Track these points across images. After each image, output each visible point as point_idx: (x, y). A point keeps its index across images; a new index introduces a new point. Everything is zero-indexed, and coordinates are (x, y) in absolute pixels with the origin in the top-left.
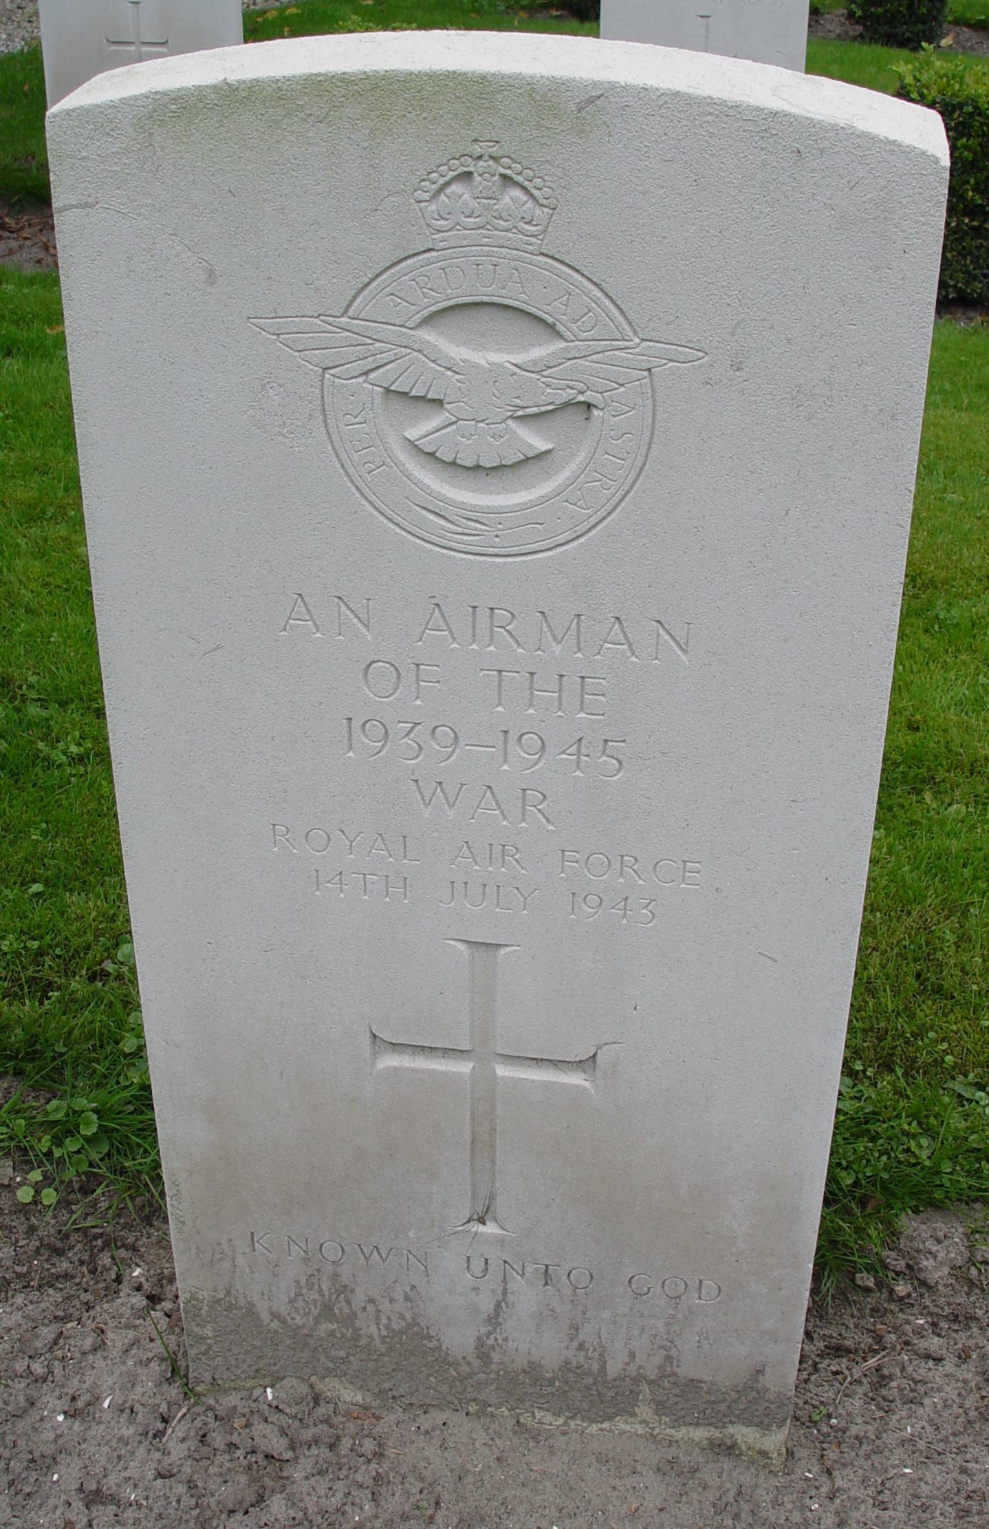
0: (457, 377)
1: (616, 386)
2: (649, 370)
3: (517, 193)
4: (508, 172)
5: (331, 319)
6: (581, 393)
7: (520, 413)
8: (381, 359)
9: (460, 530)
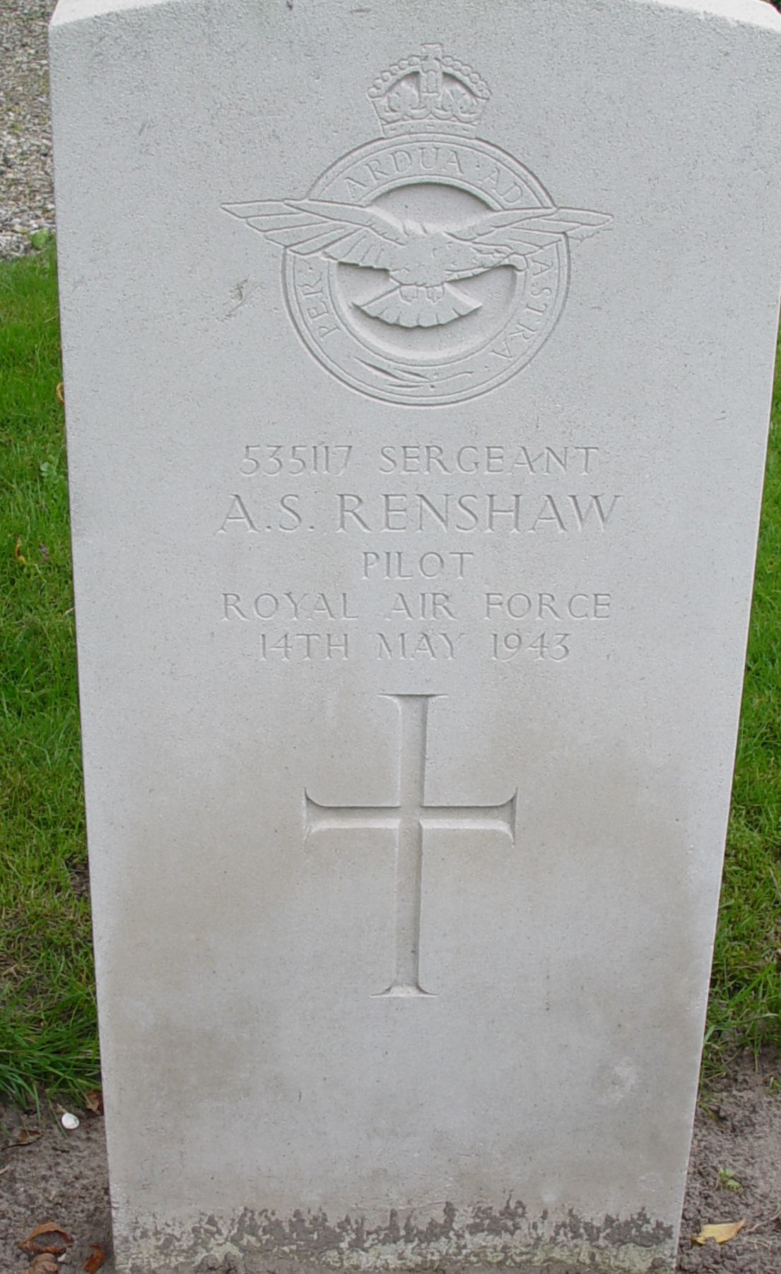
3: (458, 87)
4: (450, 70)
5: (292, 202)
7: (455, 276)
8: (337, 234)
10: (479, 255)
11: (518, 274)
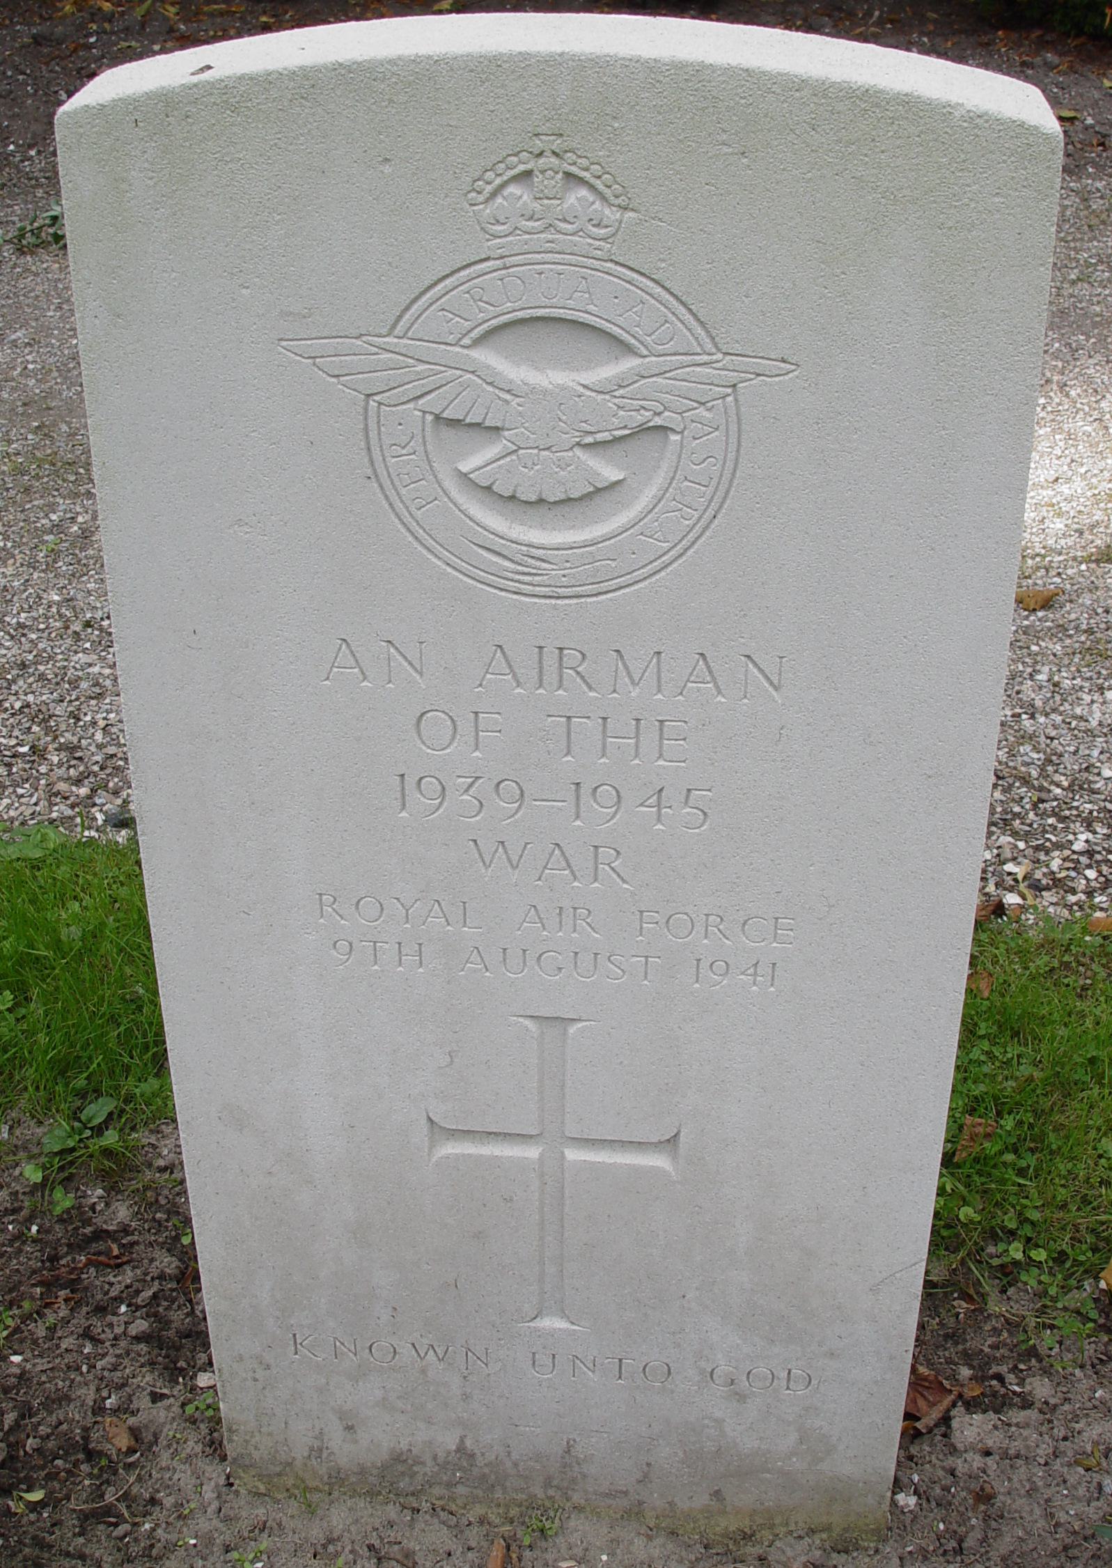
0: (518, 400)
1: (695, 405)
2: (734, 386)
3: (583, 192)
4: (573, 169)
6: (659, 414)
7: (589, 440)
8: (428, 383)
10: (621, 413)
11: (674, 438)
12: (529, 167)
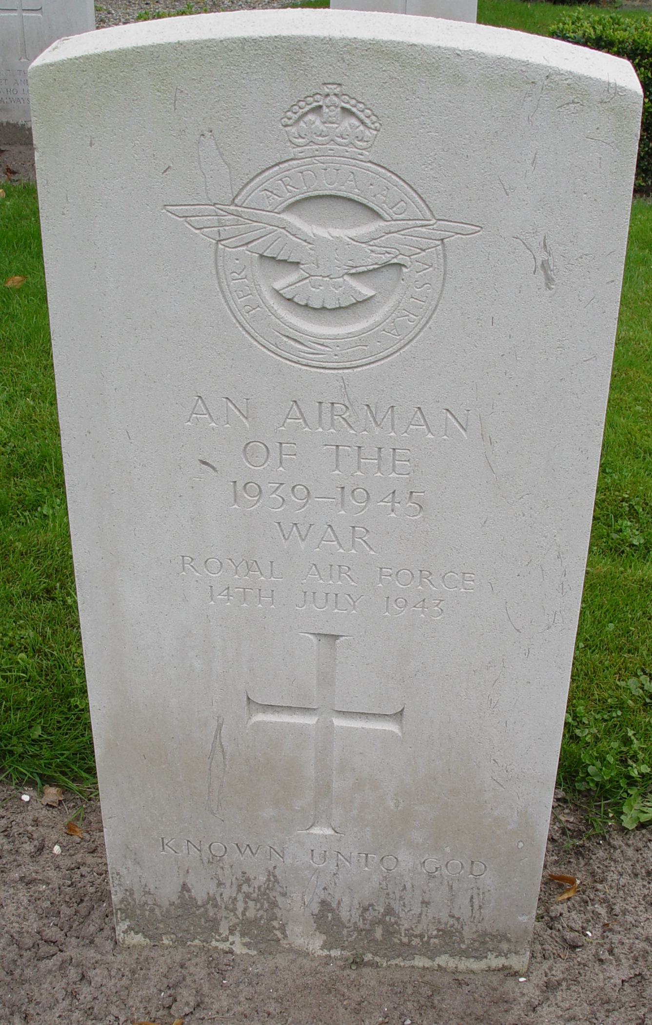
2: (442, 240)
4: (348, 106)
7: (353, 271)
9: (312, 351)
11: (405, 270)
12: (321, 103)
